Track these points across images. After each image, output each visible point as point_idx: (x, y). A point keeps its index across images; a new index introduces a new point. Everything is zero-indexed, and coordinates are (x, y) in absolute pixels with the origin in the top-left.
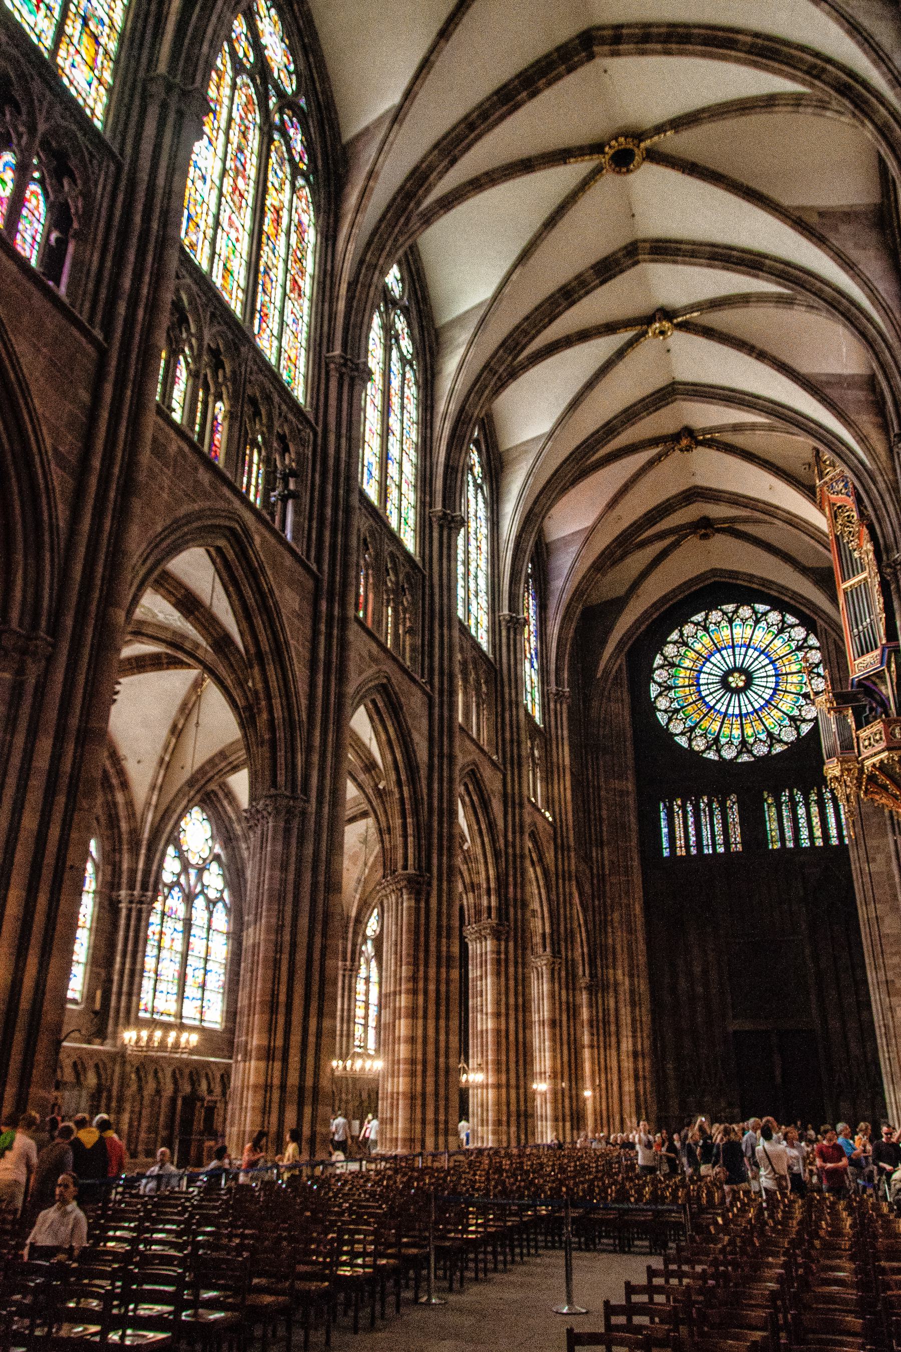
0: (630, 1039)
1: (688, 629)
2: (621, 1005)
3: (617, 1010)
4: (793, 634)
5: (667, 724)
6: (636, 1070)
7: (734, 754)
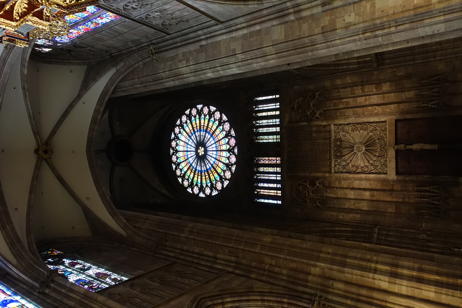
0: (376, 276)
1: (178, 173)
2: (341, 276)
3: (347, 283)
4: (184, 122)
5: (218, 190)
6: (410, 278)
7: (234, 156)
